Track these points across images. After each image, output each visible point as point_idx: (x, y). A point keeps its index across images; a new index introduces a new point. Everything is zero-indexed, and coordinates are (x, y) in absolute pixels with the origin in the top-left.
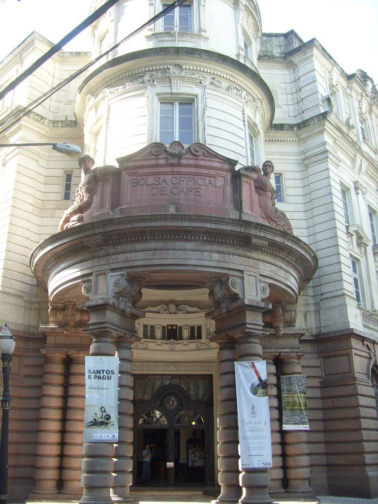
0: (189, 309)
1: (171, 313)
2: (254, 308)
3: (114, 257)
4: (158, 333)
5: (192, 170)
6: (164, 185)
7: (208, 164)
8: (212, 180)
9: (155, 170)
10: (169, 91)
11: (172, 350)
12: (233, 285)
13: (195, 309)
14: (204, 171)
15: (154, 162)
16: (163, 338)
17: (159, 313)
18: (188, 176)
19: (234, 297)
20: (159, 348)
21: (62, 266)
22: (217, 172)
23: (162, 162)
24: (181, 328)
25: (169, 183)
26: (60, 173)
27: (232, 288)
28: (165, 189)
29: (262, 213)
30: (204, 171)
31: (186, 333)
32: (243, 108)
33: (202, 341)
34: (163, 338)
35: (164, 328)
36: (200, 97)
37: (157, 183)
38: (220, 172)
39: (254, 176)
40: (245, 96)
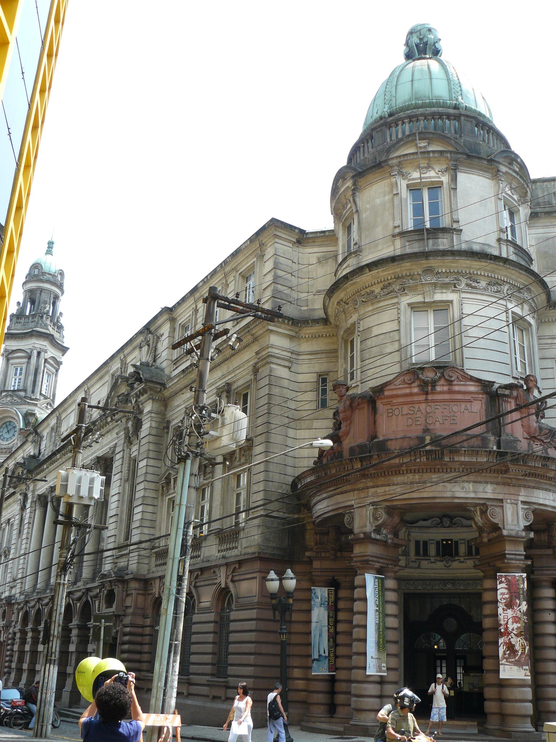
1: (444, 527)
2: (514, 539)
3: (373, 490)
4: (432, 550)
5: (447, 397)
6: (419, 414)
7: (462, 389)
8: (468, 405)
9: (409, 399)
10: (422, 300)
11: (448, 567)
12: (492, 515)
14: (459, 397)
15: (407, 391)
16: (438, 554)
18: (443, 403)
19: (496, 528)
20: (434, 565)
21: (325, 495)
22: (473, 396)
23: (416, 390)
24: (456, 543)
25: (423, 411)
26: (312, 378)
27: (490, 518)
28: (420, 419)
29: (525, 434)
30: (459, 397)
31: (462, 549)
32: (506, 306)
35: (438, 543)
36: (456, 303)
37: (412, 412)
38: (476, 396)
39: (515, 393)
40: (508, 290)
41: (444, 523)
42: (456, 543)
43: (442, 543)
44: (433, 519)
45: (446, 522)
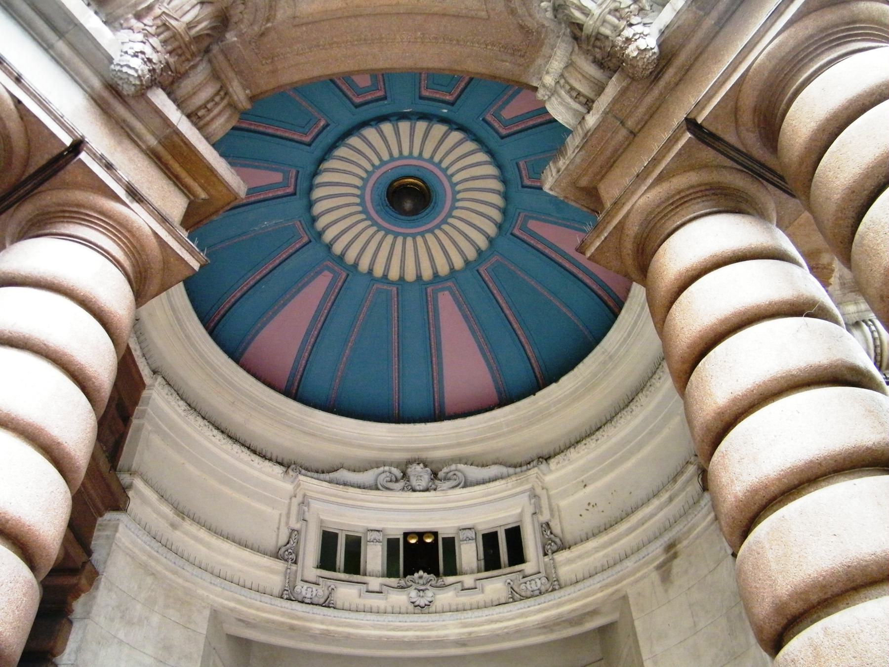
0: (474, 473)
1: (414, 490)
11: (422, 608)
13: (494, 470)
16: (391, 571)
17: (377, 489)
24: (450, 544)
33: (528, 567)
34: (391, 571)
35: (392, 544)
41: (414, 482)
42: (450, 544)
43: (406, 542)
44: (382, 469)
45: (419, 475)
